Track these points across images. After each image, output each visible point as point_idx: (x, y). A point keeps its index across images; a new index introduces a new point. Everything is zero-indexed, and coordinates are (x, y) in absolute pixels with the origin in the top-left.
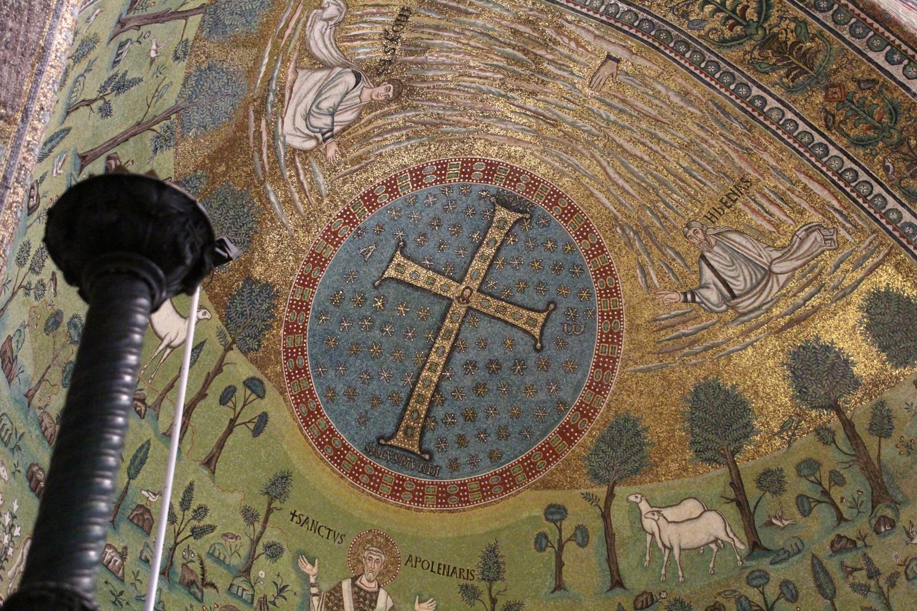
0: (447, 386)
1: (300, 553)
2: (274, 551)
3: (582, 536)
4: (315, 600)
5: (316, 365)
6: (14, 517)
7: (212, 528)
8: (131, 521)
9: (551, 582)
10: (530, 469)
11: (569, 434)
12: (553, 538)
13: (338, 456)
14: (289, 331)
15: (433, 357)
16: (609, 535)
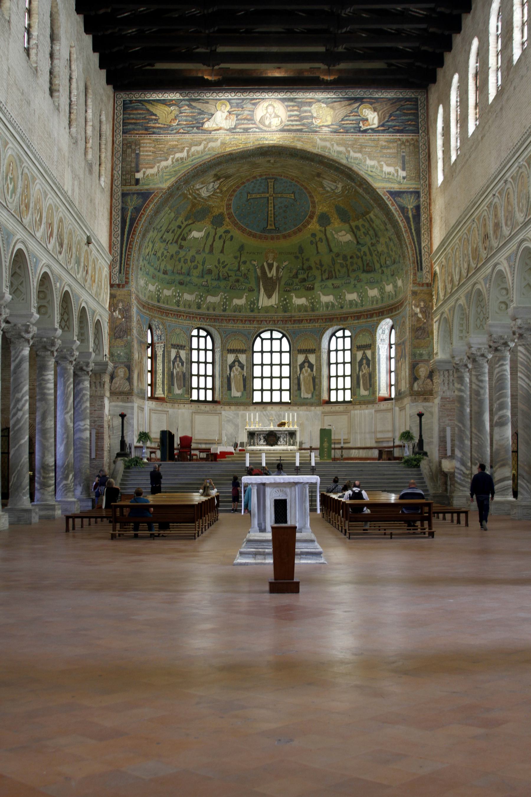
0: (277, 213)
1: (251, 260)
2: (245, 263)
3: (321, 240)
4: (258, 270)
5: (240, 221)
6: (179, 293)
7: (227, 264)
8: (207, 274)
9: (316, 252)
10: (305, 226)
11: (311, 217)
12: (314, 241)
13: (254, 236)
14: (229, 218)
15: (270, 209)
16: (327, 240)
